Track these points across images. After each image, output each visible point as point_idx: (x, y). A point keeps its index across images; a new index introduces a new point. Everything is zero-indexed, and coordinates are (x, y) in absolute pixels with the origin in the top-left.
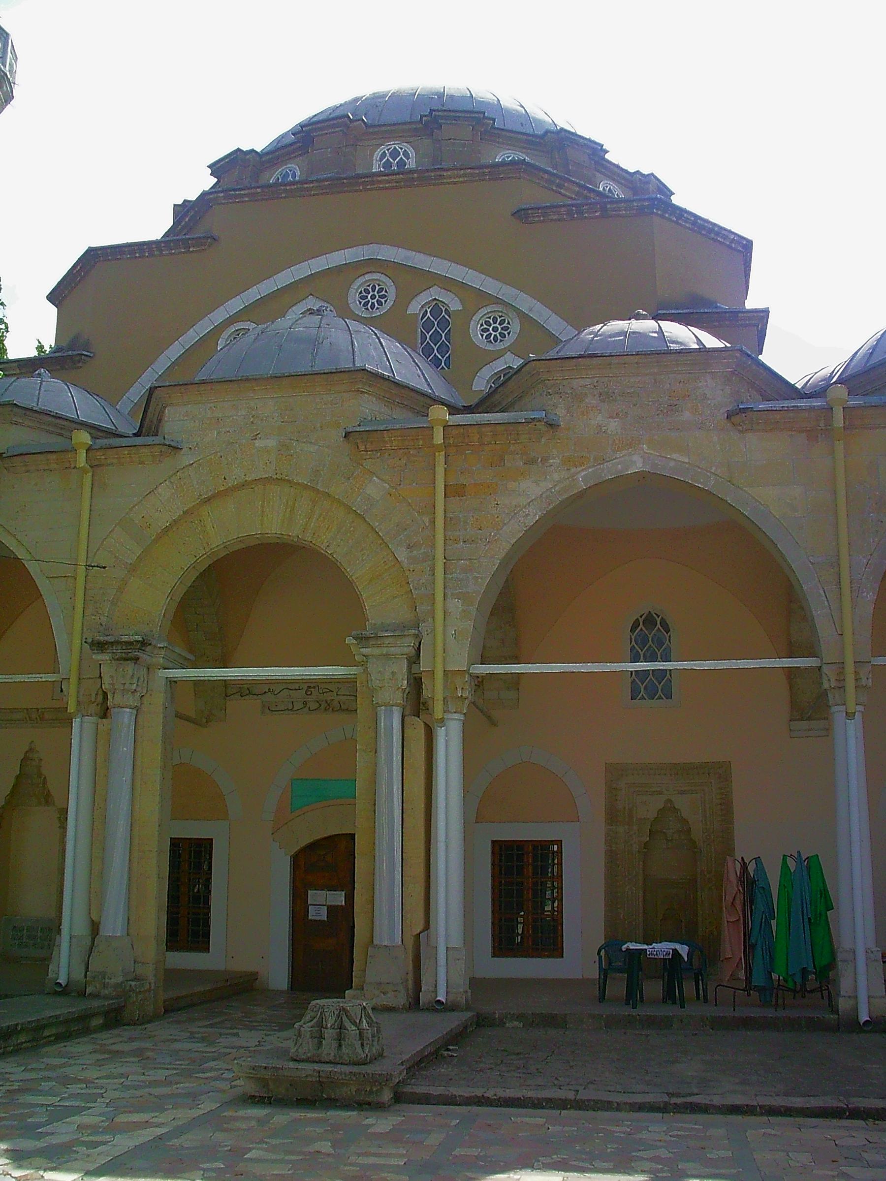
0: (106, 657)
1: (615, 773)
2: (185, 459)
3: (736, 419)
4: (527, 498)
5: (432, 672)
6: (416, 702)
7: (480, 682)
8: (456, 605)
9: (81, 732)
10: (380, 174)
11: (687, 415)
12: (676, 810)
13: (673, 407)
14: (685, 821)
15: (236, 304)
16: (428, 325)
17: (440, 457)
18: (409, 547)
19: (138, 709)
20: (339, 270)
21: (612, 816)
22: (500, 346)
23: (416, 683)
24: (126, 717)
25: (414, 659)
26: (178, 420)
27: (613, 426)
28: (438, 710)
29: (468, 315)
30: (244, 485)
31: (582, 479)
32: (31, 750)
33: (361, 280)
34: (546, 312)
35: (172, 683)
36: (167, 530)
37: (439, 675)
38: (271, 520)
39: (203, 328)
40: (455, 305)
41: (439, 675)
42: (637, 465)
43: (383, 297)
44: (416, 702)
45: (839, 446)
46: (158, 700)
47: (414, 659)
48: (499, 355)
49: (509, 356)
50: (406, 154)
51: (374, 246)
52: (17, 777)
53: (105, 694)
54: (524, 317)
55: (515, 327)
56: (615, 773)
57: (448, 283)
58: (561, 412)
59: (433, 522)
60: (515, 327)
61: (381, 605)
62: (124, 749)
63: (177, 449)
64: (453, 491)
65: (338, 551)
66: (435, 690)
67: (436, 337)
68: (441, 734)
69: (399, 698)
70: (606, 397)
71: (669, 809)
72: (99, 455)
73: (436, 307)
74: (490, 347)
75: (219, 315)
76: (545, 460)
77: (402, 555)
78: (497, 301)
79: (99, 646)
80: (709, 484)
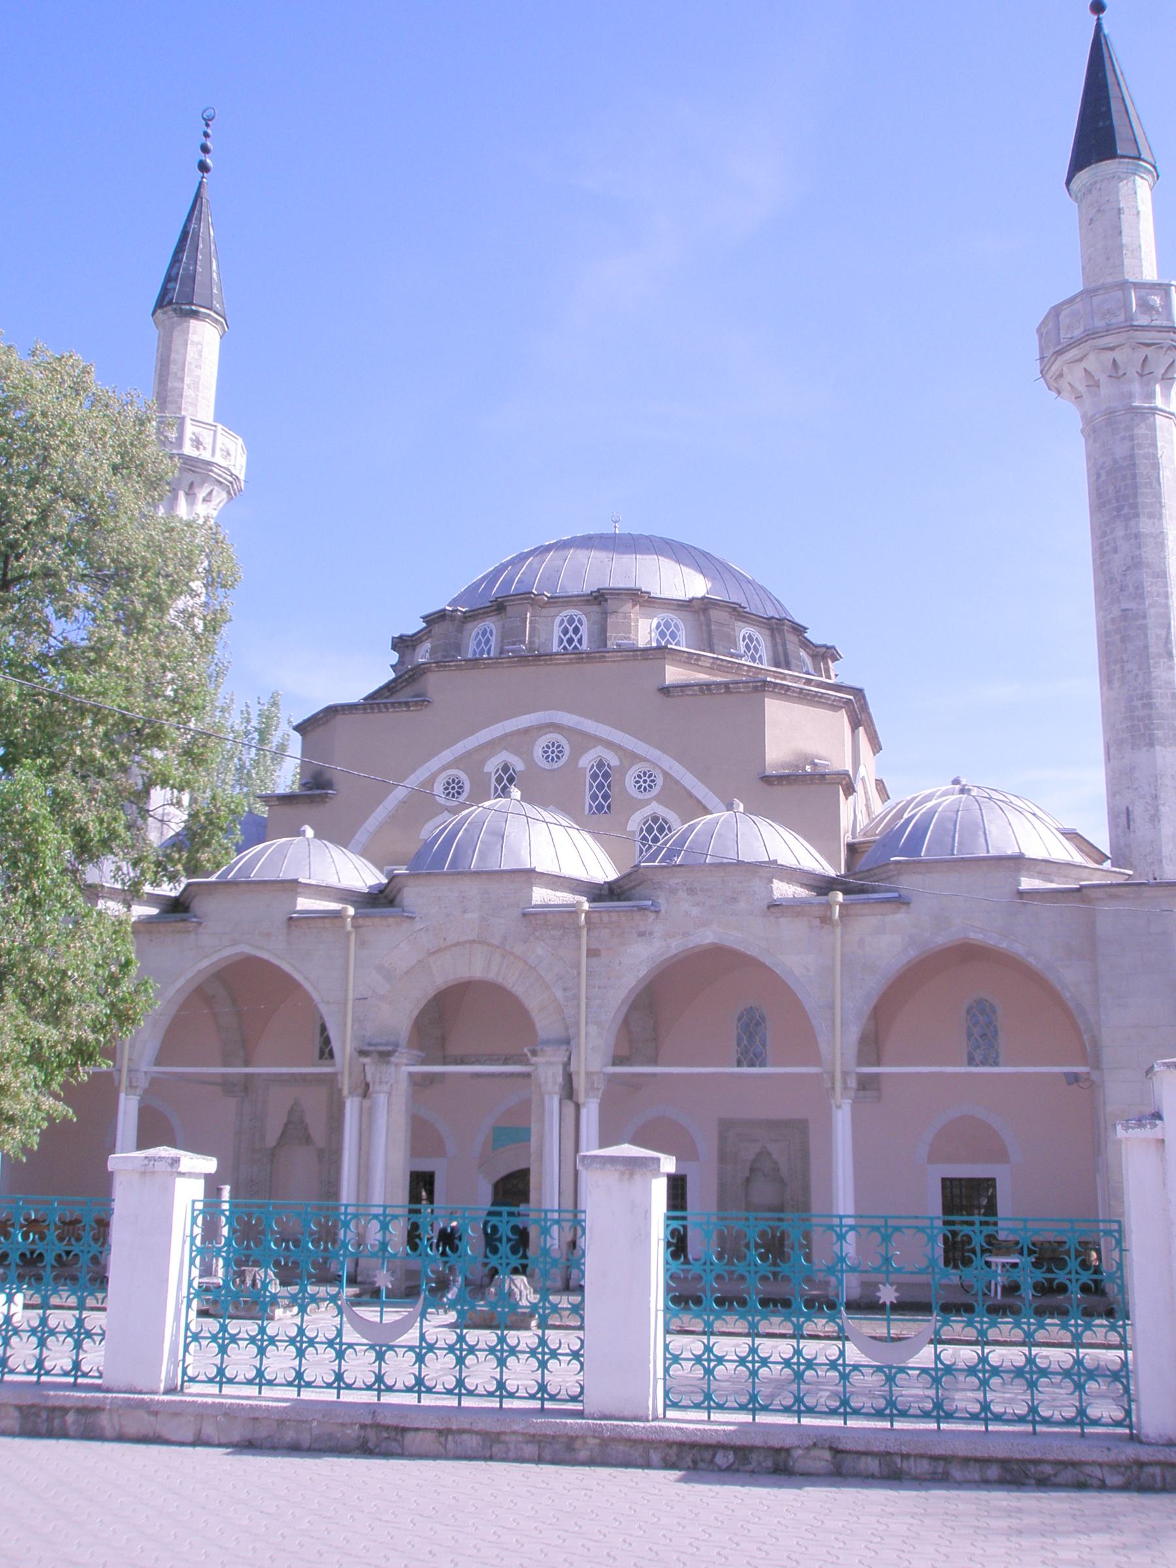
0: (367, 1060)
1: (725, 1126)
2: (418, 925)
3: (772, 910)
4: (639, 956)
5: (578, 1073)
6: (569, 1091)
7: (611, 1078)
8: (593, 1030)
9: (351, 1107)
10: (557, 654)
11: (742, 905)
12: (769, 1154)
13: (734, 900)
14: (775, 1163)
15: (447, 755)
16: (594, 776)
17: (584, 932)
18: (565, 990)
19: (390, 1094)
20: (526, 731)
21: (722, 1158)
22: (647, 795)
23: (569, 1078)
24: (382, 1099)
25: (567, 1064)
26: (411, 896)
27: (695, 911)
28: (582, 1099)
29: (623, 770)
30: (455, 945)
31: (676, 946)
32: (295, 1104)
33: (544, 738)
34: (682, 770)
35: (410, 1074)
36: (407, 973)
37: (583, 1075)
38: (476, 968)
39: (423, 773)
40: (613, 760)
41: (583, 1075)
42: (707, 937)
43: (560, 752)
44: (569, 1091)
45: (839, 930)
46: (403, 1087)
47: (567, 1064)
48: (647, 802)
49: (654, 804)
50: (580, 621)
51: (554, 712)
52: (286, 1125)
53: (367, 1085)
54: (666, 774)
55: (660, 781)
56: (725, 1126)
57: (610, 745)
58: (661, 901)
59: (579, 974)
60: (660, 781)
61: (545, 1025)
62: (381, 1120)
63: (412, 918)
64: (592, 953)
65: (519, 991)
66: (580, 1084)
67: (600, 787)
68: (583, 1111)
69: (557, 1089)
70: (691, 891)
71: (764, 1154)
72: (361, 921)
73: (601, 765)
74: (640, 796)
75: (434, 764)
76: (651, 933)
77: (560, 995)
78: (646, 760)
79: (363, 1053)
80: (753, 951)
